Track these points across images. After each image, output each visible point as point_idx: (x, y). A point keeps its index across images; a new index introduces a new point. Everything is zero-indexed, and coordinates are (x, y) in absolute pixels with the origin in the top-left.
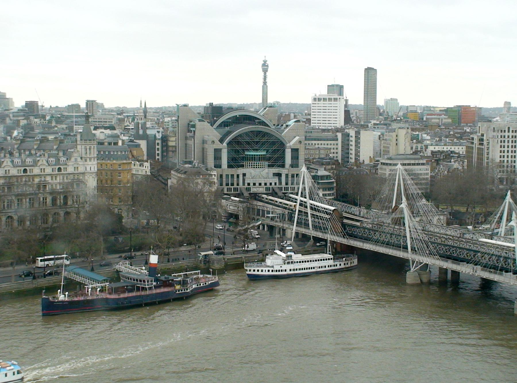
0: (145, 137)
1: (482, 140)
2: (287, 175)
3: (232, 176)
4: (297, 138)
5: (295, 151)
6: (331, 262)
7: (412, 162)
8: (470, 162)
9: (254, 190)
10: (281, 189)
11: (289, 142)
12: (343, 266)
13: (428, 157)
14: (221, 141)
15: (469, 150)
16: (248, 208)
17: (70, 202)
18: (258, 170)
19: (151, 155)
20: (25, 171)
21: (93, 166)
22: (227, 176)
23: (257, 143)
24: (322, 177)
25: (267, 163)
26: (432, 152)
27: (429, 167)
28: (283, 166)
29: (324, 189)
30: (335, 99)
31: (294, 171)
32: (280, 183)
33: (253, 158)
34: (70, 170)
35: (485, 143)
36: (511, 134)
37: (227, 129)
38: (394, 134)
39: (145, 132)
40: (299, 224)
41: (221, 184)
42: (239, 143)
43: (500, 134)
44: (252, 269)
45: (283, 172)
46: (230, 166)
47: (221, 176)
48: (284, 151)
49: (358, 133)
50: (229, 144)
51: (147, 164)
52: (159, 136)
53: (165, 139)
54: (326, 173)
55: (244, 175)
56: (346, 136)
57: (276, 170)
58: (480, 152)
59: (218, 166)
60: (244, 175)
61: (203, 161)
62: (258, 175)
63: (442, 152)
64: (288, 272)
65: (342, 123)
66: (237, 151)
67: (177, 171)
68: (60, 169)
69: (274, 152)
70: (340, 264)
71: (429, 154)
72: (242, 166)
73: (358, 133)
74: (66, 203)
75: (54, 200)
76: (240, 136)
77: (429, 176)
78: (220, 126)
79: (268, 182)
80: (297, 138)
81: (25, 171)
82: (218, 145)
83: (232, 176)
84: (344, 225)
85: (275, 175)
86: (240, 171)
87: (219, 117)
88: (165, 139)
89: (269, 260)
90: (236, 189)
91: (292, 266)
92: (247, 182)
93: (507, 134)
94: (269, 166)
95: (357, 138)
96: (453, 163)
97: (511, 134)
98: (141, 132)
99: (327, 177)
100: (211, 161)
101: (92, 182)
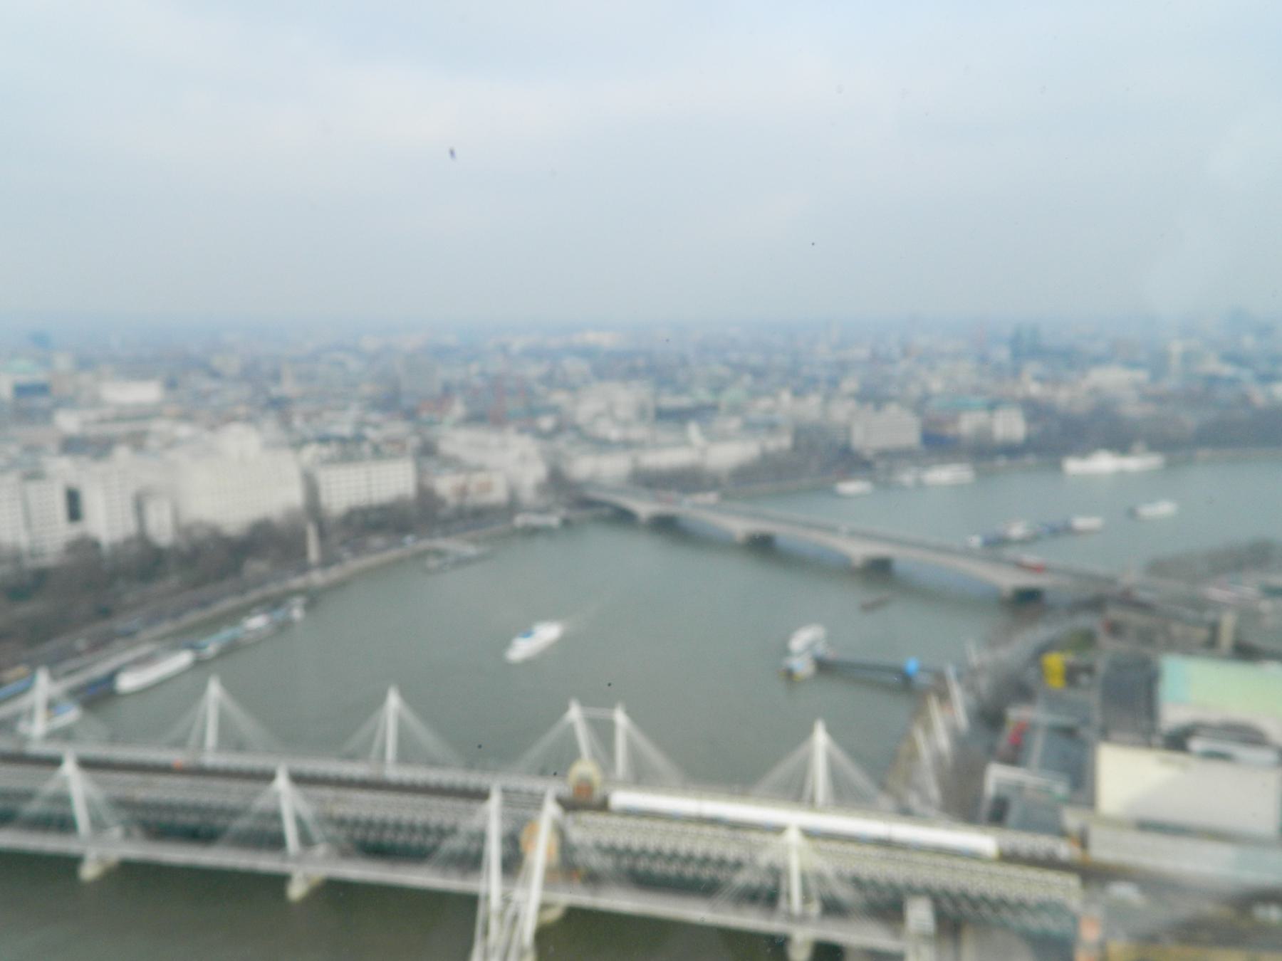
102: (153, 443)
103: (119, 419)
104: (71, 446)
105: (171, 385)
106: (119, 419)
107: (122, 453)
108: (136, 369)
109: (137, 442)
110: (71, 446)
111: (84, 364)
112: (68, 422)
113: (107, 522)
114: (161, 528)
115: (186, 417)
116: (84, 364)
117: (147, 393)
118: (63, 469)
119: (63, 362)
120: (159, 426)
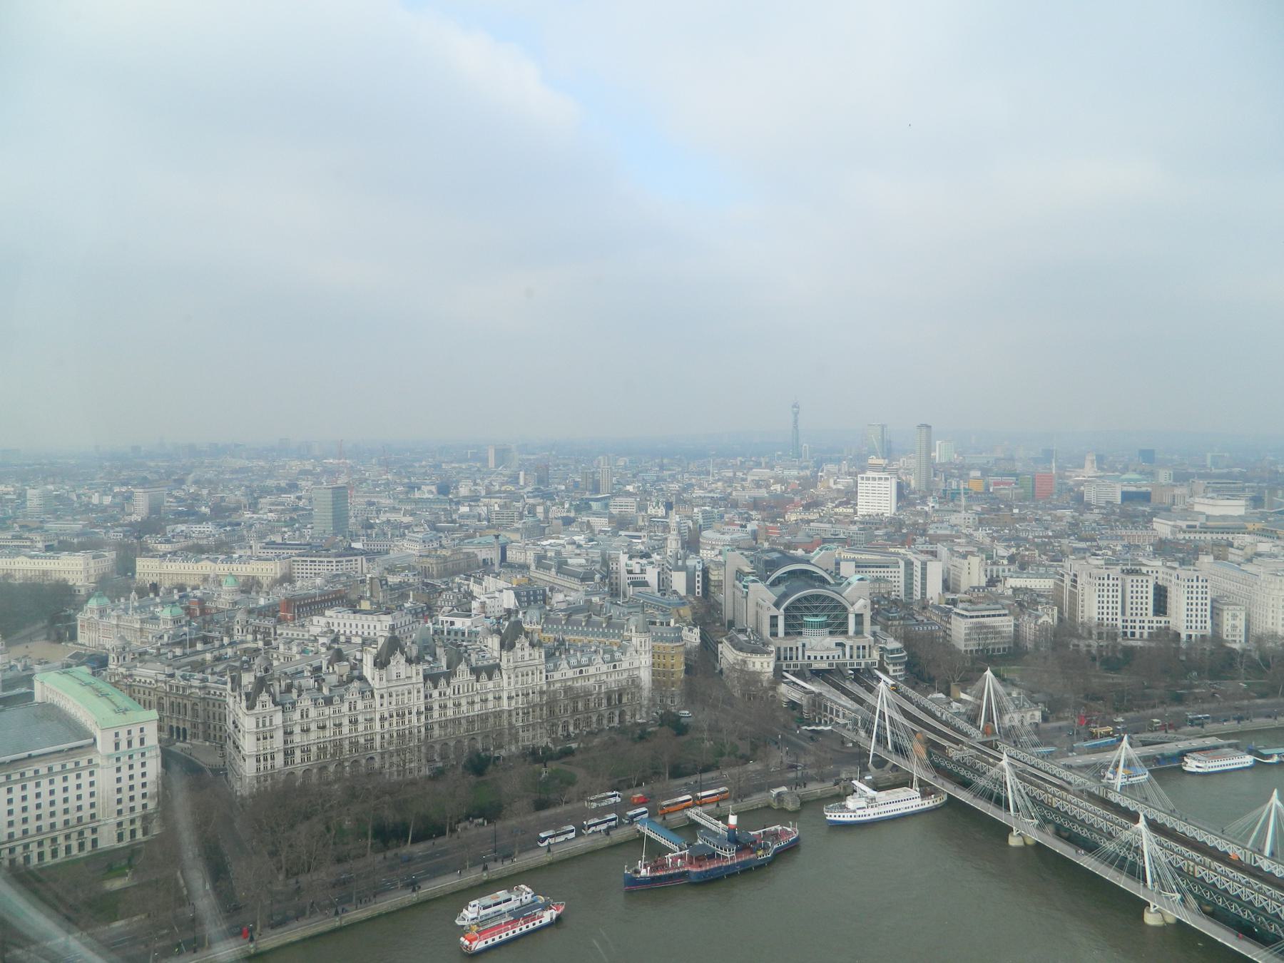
0: (684, 568)
1: (1075, 581)
2: (851, 648)
3: (791, 649)
4: (861, 602)
5: (859, 617)
6: (919, 801)
7: (993, 613)
8: (1060, 612)
9: (816, 666)
10: (845, 665)
11: (853, 604)
12: (931, 804)
13: (1007, 598)
14: (777, 605)
15: (1059, 588)
16: (814, 701)
17: (624, 700)
18: (818, 638)
19: (690, 588)
20: (581, 672)
21: (645, 660)
22: (785, 650)
23: (817, 607)
24: (892, 652)
25: (828, 630)
26: (1015, 590)
27: (1012, 618)
28: (846, 632)
29: (895, 665)
30: (886, 479)
31: (861, 642)
32: (844, 654)
33: (812, 625)
34: (625, 665)
35: (1079, 587)
36: (1111, 582)
37: (782, 588)
38: (966, 562)
39: (684, 562)
40: (878, 741)
41: (779, 659)
42: (797, 609)
43: (1098, 582)
44: (833, 816)
45: (848, 643)
46: (787, 634)
47: (779, 649)
48: (847, 618)
49: (924, 564)
50: (786, 610)
51: (697, 630)
52: (699, 567)
53: (705, 571)
54: (897, 645)
55: (804, 645)
56: (909, 564)
57: (841, 639)
58: (1073, 596)
59: (774, 634)
60: (804, 645)
61: (757, 631)
62: (819, 646)
63: (1026, 590)
64: (872, 817)
65: (893, 510)
66: (794, 617)
67: (731, 640)
68: (615, 667)
69: (836, 617)
70: (929, 803)
71: (1010, 592)
72: (800, 633)
73: (924, 564)
74: (620, 701)
75: (609, 699)
76: (799, 600)
77: (1012, 629)
78: (773, 584)
79: (831, 654)
80: (861, 602)
81: (581, 672)
82: (774, 612)
83: (791, 649)
84: (929, 754)
85: (837, 644)
86: (799, 642)
87: (772, 571)
88: (705, 571)
89: (851, 803)
90: (795, 666)
91: (876, 810)
92: (807, 654)
93: (1106, 582)
94: (831, 633)
95: (924, 570)
96: (1040, 612)
97: (1111, 582)
98: (680, 563)
99: (898, 651)
100: (766, 630)
101: (645, 677)
102: (1234, 555)
103: (1205, 529)
104: (1163, 548)
105: (1257, 501)
106: (1205, 529)
107: (1206, 560)
108: (1225, 485)
109: (1220, 551)
110: (1163, 548)
111: (1181, 478)
112: (1163, 528)
113: (1186, 618)
114: (1234, 631)
115: (1264, 533)
116: (1181, 478)
117: (1235, 508)
118: (1156, 568)
119: (1164, 476)
120: (1239, 539)
